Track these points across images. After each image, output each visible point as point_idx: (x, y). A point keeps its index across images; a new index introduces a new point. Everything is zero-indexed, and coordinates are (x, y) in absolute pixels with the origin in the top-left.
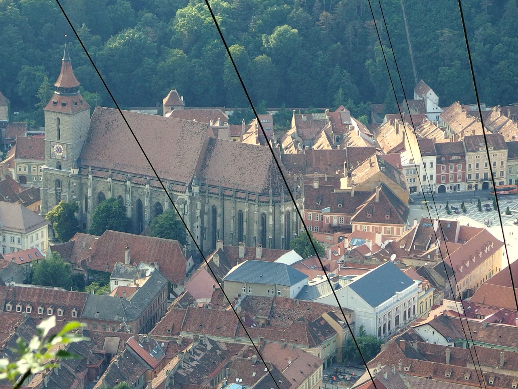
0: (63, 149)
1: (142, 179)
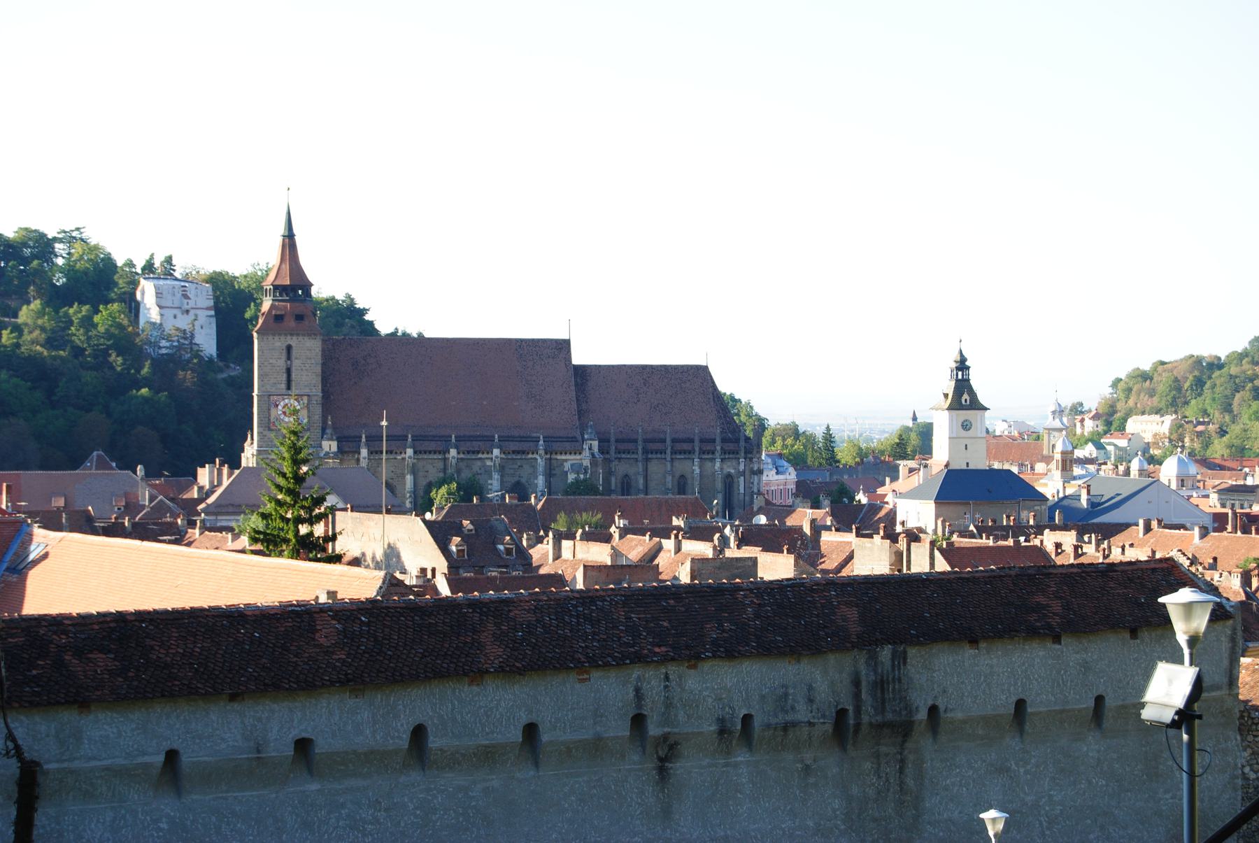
1: (479, 443)
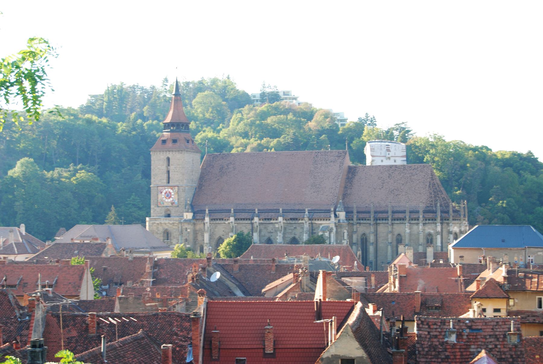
0: (173, 194)
1: (273, 214)
